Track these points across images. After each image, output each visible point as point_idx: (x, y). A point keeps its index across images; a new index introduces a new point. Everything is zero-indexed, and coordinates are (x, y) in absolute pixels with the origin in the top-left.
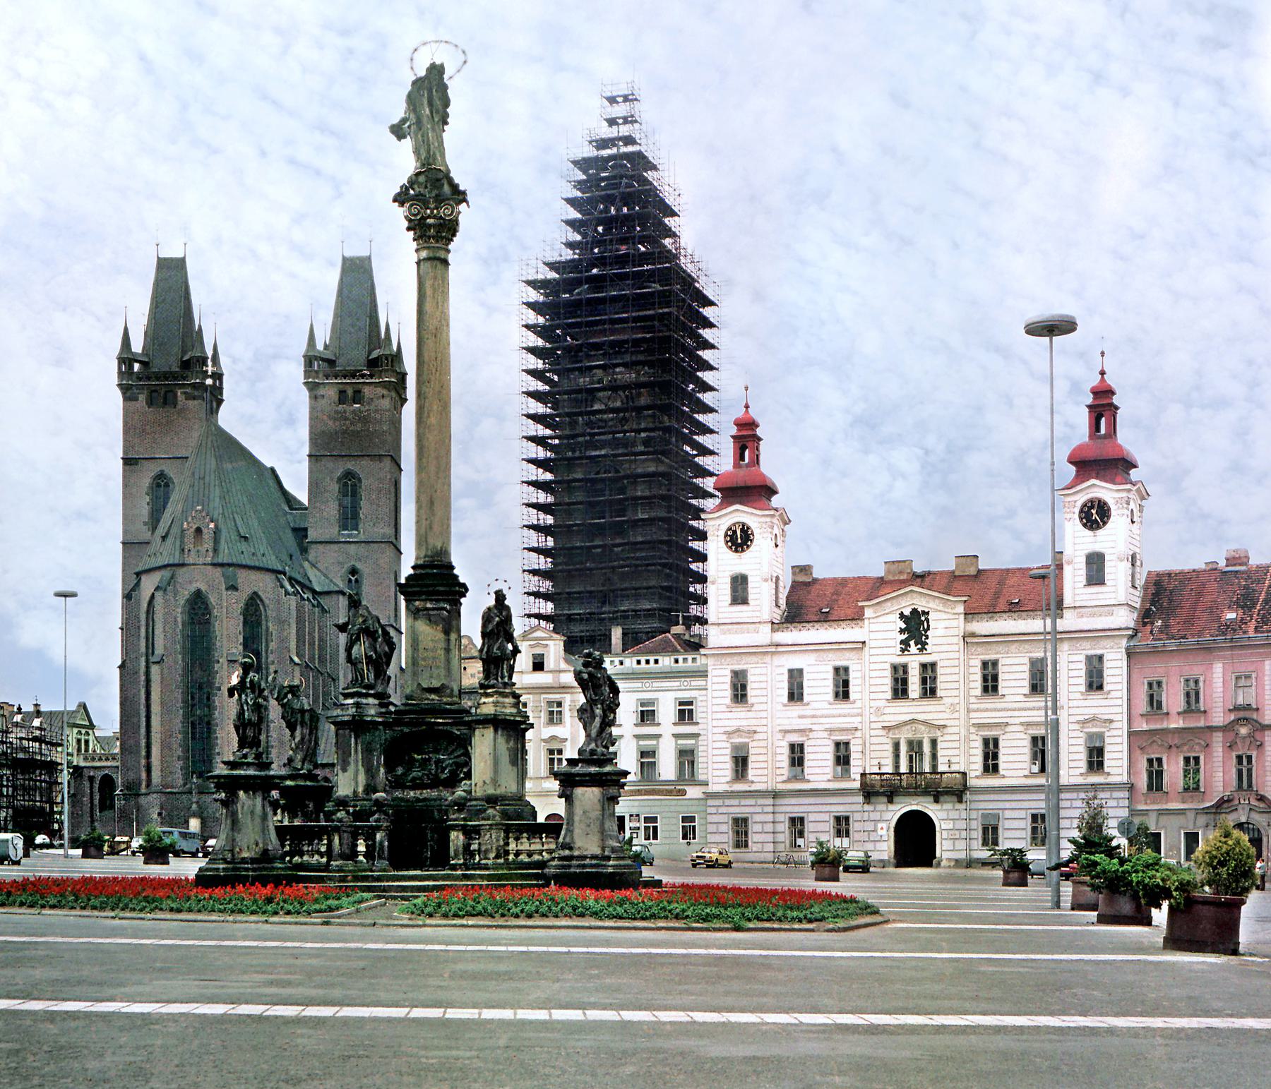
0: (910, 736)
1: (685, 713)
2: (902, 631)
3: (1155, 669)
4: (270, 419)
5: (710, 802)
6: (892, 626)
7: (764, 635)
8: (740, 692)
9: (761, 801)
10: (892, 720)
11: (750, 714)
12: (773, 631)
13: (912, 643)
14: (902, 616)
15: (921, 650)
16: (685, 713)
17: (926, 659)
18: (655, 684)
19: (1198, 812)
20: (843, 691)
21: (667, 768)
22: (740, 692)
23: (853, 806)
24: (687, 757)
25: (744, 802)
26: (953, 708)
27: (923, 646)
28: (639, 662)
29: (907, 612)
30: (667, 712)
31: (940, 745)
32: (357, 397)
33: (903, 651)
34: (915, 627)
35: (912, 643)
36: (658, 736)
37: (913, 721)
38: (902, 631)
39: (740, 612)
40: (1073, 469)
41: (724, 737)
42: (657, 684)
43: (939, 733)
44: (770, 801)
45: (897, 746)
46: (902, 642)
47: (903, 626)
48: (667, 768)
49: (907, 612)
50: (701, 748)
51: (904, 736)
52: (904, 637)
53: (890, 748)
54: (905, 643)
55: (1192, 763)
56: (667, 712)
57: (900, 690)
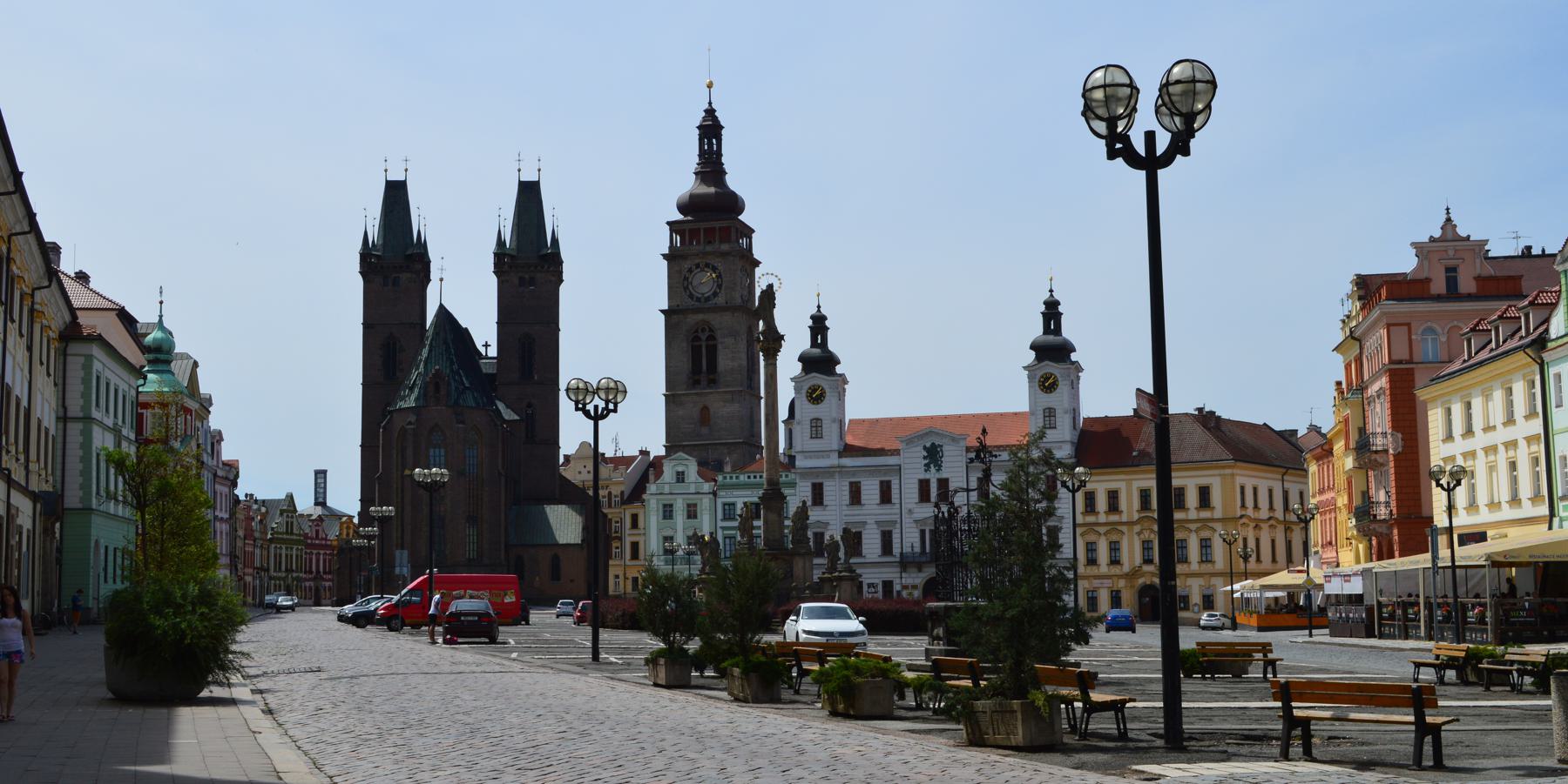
4: (466, 293)
7: (834, 460)
12: (840, 456)
19: (1120, 577)
20: (886, 497)
23: (891, 574)
32: (532, 281)
34: (933, 455)
39: (816, 445)
40: (1032, 354)
45: (923, 532)
54: (927, 465)
55: (1114, 548)
57: (924, 496)
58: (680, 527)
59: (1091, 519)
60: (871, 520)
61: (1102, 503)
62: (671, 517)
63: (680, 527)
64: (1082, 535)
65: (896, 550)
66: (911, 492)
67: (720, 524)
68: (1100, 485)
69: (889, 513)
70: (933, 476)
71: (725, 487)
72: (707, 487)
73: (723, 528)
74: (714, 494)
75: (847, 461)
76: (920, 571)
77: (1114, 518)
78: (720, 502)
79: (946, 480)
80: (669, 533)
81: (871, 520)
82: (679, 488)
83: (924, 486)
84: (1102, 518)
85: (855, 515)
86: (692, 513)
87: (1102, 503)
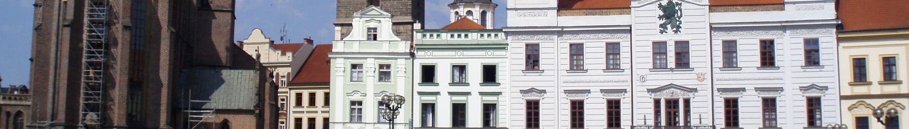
0: (669, 97)
1: (490, 74)
2: (660, 17)
3: (859, 49)
7: (552, 19)
8: (533, 61)
13: (669, 26)
15: (676, 32)
16: (490, 74)
17: (681, 37)
22: (533, 61)
26: (701, 78)
27: (677, 29)
28: (452, 36)
31: (692, 105)
33: (662, 32)
37: (671, 86)
38: (660, 17)
41: (520, 95)
42: (466, 53)
45: (657, 103)
46: (661, 26)
50: (500, 103)
51: (663, 97)
53: (652, 105)
56: (475, 74)
58: (370, 91)
59: (861, 90)
60: (595, 89)
61: (875, 71)
62: (360, 80)
63: (370, 91)
64: (850, 109)
66: (644, 57)
67: (418, 88)
68: (874, 52)
69: (615, 80)
70: (670, 38)
71: (423, 47)
72: (403, 47)
73: (420, 93)
74: (412, 55)
75: (570, 20)
77: (890, 89)
79: (686, 43)
80: (356, 97)
81: (595, 89)
82: (372, 47)
83: (659, 49)
84: (875, 89)
85: (577, 81)
86: (384, 74)
87: (875, 71)
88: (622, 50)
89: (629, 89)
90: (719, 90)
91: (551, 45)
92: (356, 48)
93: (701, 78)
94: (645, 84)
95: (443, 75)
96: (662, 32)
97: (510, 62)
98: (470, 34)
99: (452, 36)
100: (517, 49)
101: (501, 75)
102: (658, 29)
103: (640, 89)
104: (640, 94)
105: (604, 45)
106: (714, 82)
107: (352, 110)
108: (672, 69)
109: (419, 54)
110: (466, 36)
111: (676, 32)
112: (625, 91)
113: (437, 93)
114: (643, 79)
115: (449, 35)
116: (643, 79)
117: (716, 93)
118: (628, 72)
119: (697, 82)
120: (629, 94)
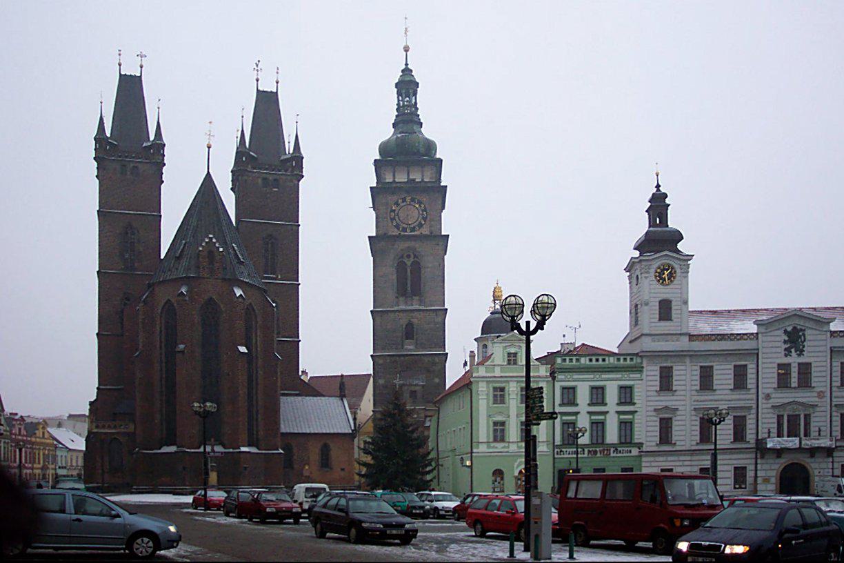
0: (791, 413)
1: (626, 394)
5: (644, 459)
6: (778, 339)
7: (684, 344)
8: (666, 382)
9: (682, 458)
10: (773, 401)
11: (675, 398)
14: (785, 331)
15: (799, 355)
16: (626, 394)
18: (603, 376)
20: (740, 379)
21: (612, 436)
22: (666, 382)
23: (746, 460)
24: (626, 427)
25: (670, 458)
28: (591, 360)
29: (789, 329)
30: (612, 395)
31: (812, 419)
33: (786, 355)
34: (795, 340)
35: (793, 350)
36: (605, 413)
39: (665, 327)
43: (811, 409)
44: (689, 458)
45: (780, 418)
46: (786, 349)
47: (787, 338)
48: (612, 436)
49: (789, 329)
50: (636, 421)
52: (787, 346)
56: (612, 395)
57: (783, 381)
62: (503, 402)
65: (750, 436)
66: (769, 378)
69: (744, 399)
74: (554, 378)
76: (779, 456)
78: (558, 385)
80: (499, 418)
85: (709, 401)
88: (749, 371)
89: (754, 406)
90: (836, 405)
91: (683, 368)
92: (497, 372)
93: (821, 395)
94: (770, 401)
95: (583, 395)
96: (786, 355)
97: (646, 384)
98: (607, 358)
99: (591, 360)
100: (652, 373)
101: (638, 395)
102: (783, 353)
103: (764, 406)
104: (765, 411)
105: (732, 367)
106: (833, 399)
107: (495, 431)
108: (795, 388)
109: (560, 377)
110: (604, 360)
111: (799, 355)
112: (750, 408)
113: (577, 414)
114: (768, 397)
115: (588, 358)
116: (768, 397)
117: (834, 409)
118: (754, 391)
119: (817, 399)
120: (754, 411)
